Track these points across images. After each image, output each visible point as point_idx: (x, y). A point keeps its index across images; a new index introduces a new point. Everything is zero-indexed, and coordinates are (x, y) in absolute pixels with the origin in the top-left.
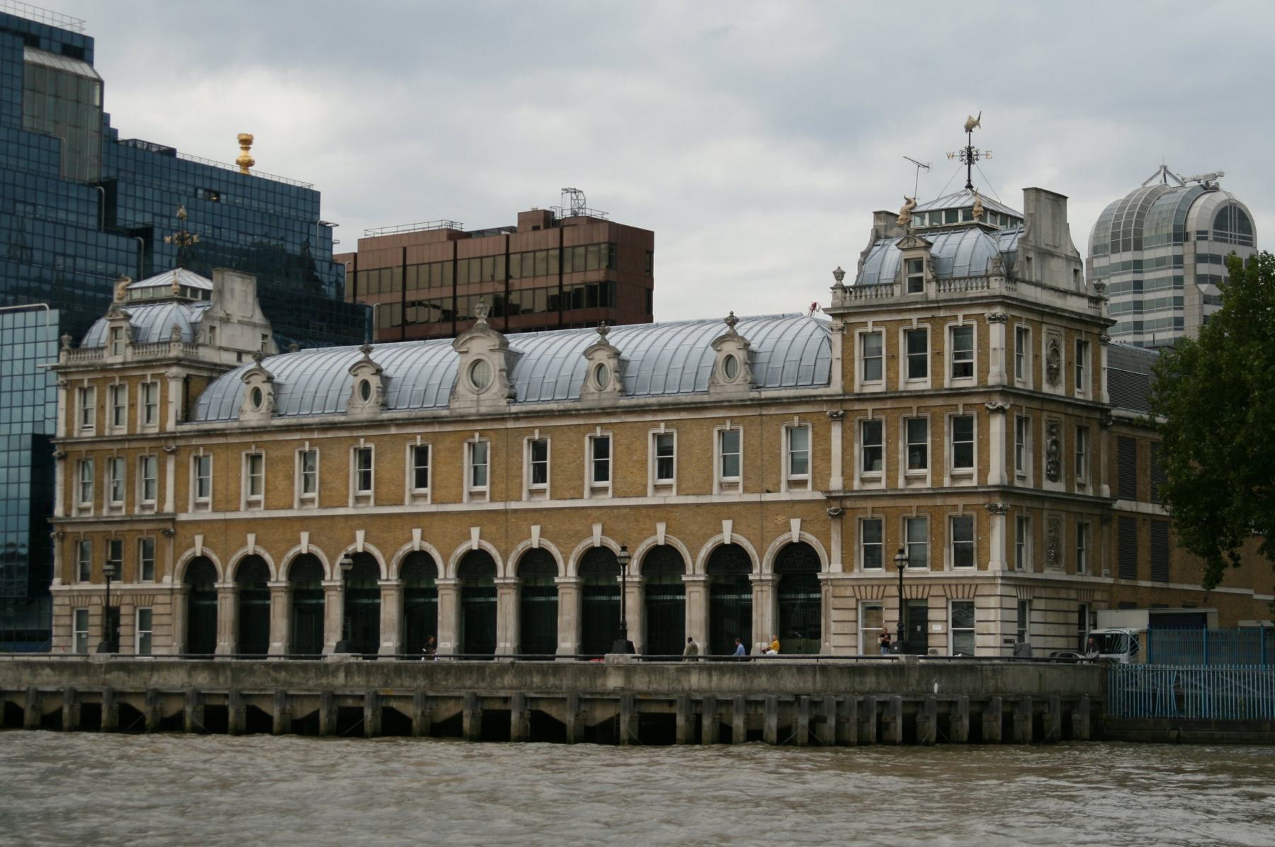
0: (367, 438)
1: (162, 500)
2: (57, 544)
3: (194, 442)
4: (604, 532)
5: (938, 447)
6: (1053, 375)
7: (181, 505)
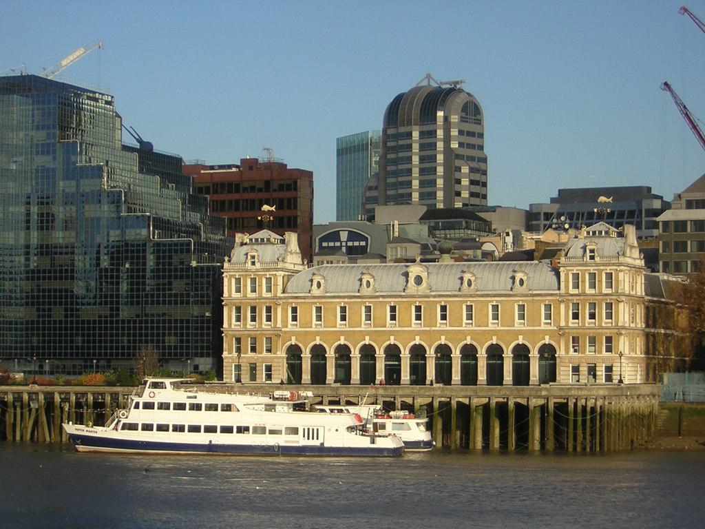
0: (369, 302)
1: (276, 322)
2: (224, 338)
3: (290, 300)
4: (471, 339)
5: (600, 313)
6: (632, 291)
7: (285, 324)
